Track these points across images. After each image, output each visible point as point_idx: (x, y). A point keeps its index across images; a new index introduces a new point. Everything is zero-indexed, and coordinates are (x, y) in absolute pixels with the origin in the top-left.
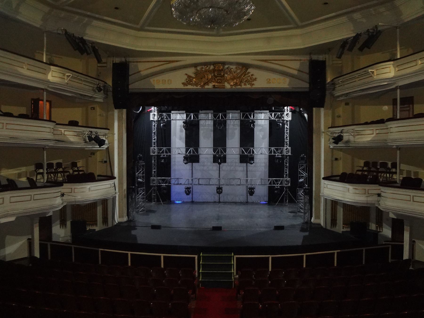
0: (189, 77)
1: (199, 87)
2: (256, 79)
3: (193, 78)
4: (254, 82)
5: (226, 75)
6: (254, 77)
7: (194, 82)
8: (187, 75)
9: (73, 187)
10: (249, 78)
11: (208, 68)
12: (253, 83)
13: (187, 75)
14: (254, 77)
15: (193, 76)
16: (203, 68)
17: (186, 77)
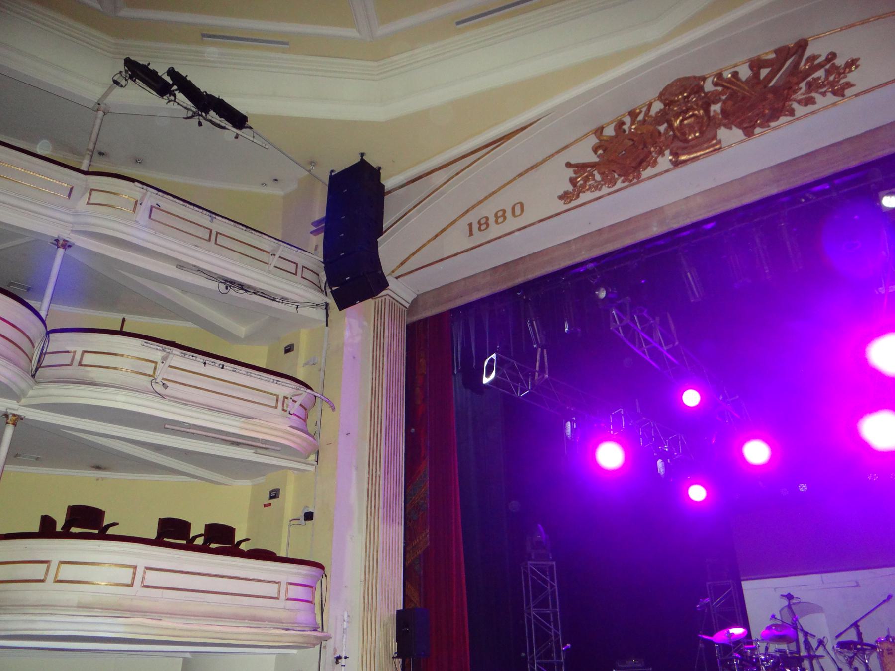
0: (580, 168)
1: (619, 185)
2: (852, 63)
3: (593, 165)
4: (851, 77)
5: (716, 108)
6: (840, 62)
7: (598, 177)
8: (569, 165)
9: (55, 559)
10: (821, 73)
11: (641, 118)
12: (843, 81)
13: (569, 165)
14: (840, 62)
15: (594, 158)
16: (623, 123)
17: (570, 173)
